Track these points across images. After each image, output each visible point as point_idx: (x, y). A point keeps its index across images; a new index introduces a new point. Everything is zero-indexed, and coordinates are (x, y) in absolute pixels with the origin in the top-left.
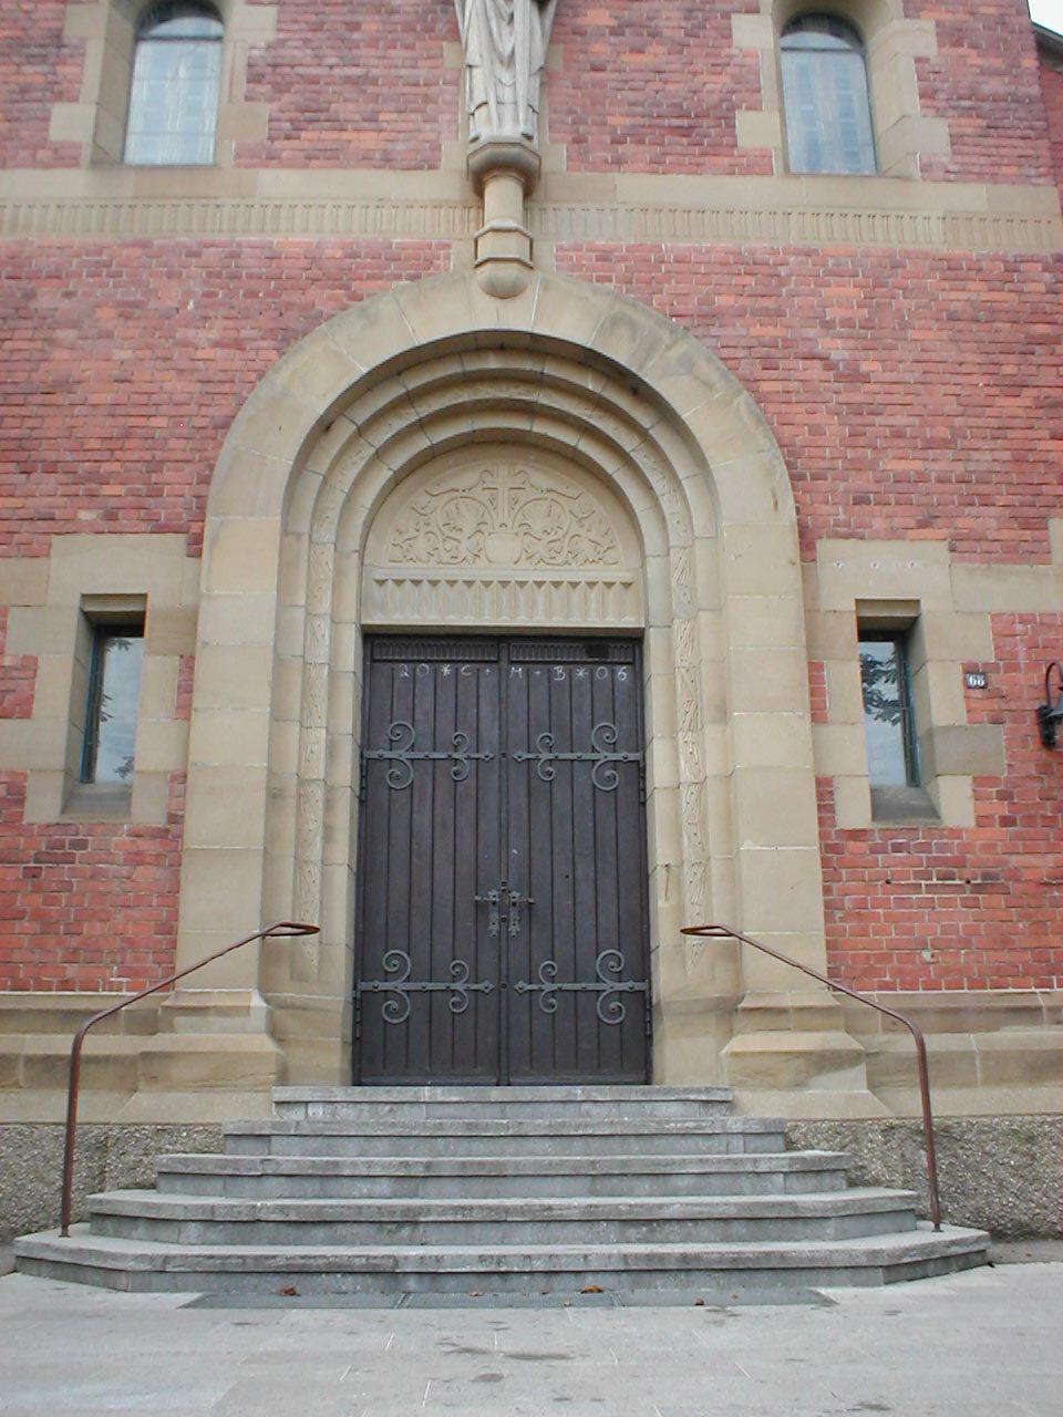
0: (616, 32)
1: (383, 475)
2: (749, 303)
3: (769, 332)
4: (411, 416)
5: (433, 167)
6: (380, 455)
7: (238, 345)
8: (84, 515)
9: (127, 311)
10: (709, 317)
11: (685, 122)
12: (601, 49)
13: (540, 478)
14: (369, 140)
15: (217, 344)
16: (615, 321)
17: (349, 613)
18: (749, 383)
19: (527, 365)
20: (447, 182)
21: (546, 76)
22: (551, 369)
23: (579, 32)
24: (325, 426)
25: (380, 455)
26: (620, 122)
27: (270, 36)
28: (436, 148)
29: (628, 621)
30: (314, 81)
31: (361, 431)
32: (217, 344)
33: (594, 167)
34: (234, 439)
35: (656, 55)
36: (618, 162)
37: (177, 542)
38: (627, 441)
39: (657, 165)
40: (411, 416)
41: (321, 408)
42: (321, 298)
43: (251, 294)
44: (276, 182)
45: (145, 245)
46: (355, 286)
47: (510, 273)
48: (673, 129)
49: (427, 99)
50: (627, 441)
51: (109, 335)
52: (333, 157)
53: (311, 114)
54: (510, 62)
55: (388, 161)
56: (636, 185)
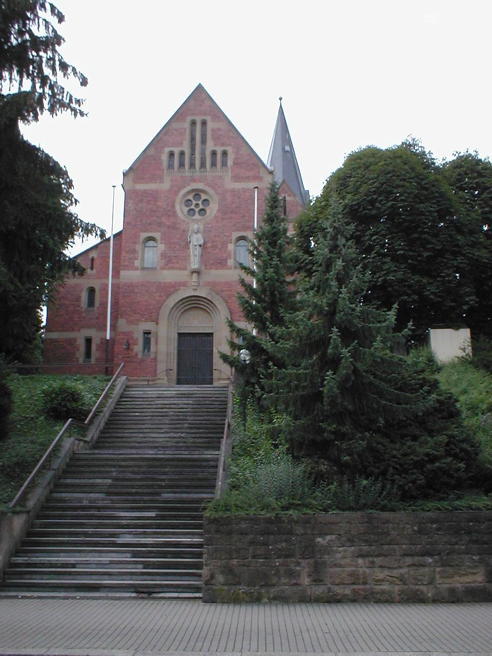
0: (211, 247)
1: (180, 313)
2: (228, 289)
3: (229, 293)
4: (183, 305)
5: (186, 269)
6: (180, 310)
7: (161, 296)
8: (143, 320)
9: (147, 291)
10: (222, 291)
11: (220, 261)
12: (209, 250)
13: (201, 312)
14: (177, 266)
15: (158, 296)
16: (209, 293)
17: (176, 331)
18: (226, 302)
19: (197, 299)
20: (187, 273)
21: (202, 256)
22: (201, 299)
23: (206, 247)
24: (173, 308)
25: (180, 310)
26: (211, 262)
27: (164, 249)
28: (186, 267)
29: (212, 332)
30: (169, 256)
31: (177, 308)
32: (158, 296)
33: (208, 269)
34: (162, 310)
35: (217, 250)
36: (211, 268)
37: (154, 323)
38: (211, 308)
39: (216, 269)
40: (183, 305)
41: (172, 306)
42: (172, 290)
43: (163, 289)
44: (165, 272)
45: (148, 282)
46: (176, 288)
47: (196, 287)
48: (219, 263)
49: (186, 259)
50: (211, 308)
51: (144, 295)
52: (173, 268)
53: (170, 261)
54: (196, 256)
55: (180, 269)
56: (214, 272)
